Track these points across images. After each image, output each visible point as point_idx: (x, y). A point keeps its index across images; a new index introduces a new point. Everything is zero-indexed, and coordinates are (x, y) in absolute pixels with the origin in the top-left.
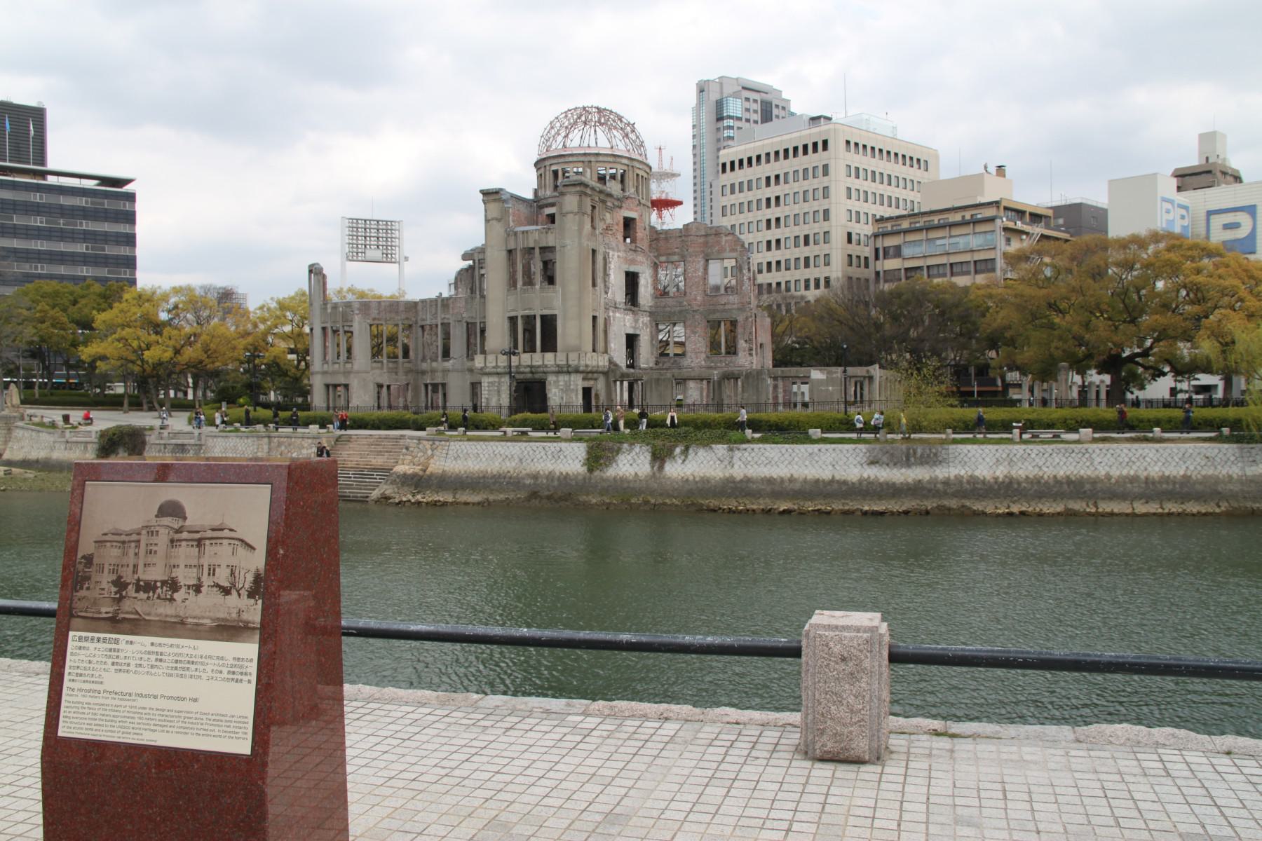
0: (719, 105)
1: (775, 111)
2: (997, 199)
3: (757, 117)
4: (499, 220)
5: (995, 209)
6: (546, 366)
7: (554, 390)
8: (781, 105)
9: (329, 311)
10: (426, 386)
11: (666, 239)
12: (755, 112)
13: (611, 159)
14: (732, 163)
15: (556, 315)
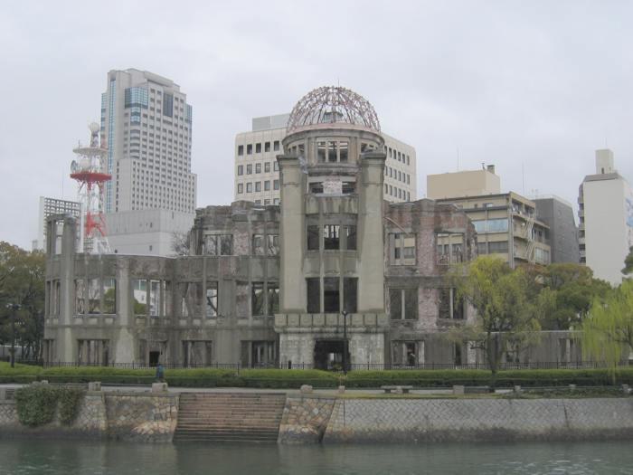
0: (128, 93)
1: (175, 103)
2: (508, 192)
3: (158, 106)
4: (297, 185)
5: (505, 200)
6: (354, 326)
7: (359, 350)
8: (180, 97)
9: (87, 263)
10: (185, 343)
11: (400, 213)
12: (159, 102)
13: (371, 137)
14: (250, 147)
15: (357, 279)
